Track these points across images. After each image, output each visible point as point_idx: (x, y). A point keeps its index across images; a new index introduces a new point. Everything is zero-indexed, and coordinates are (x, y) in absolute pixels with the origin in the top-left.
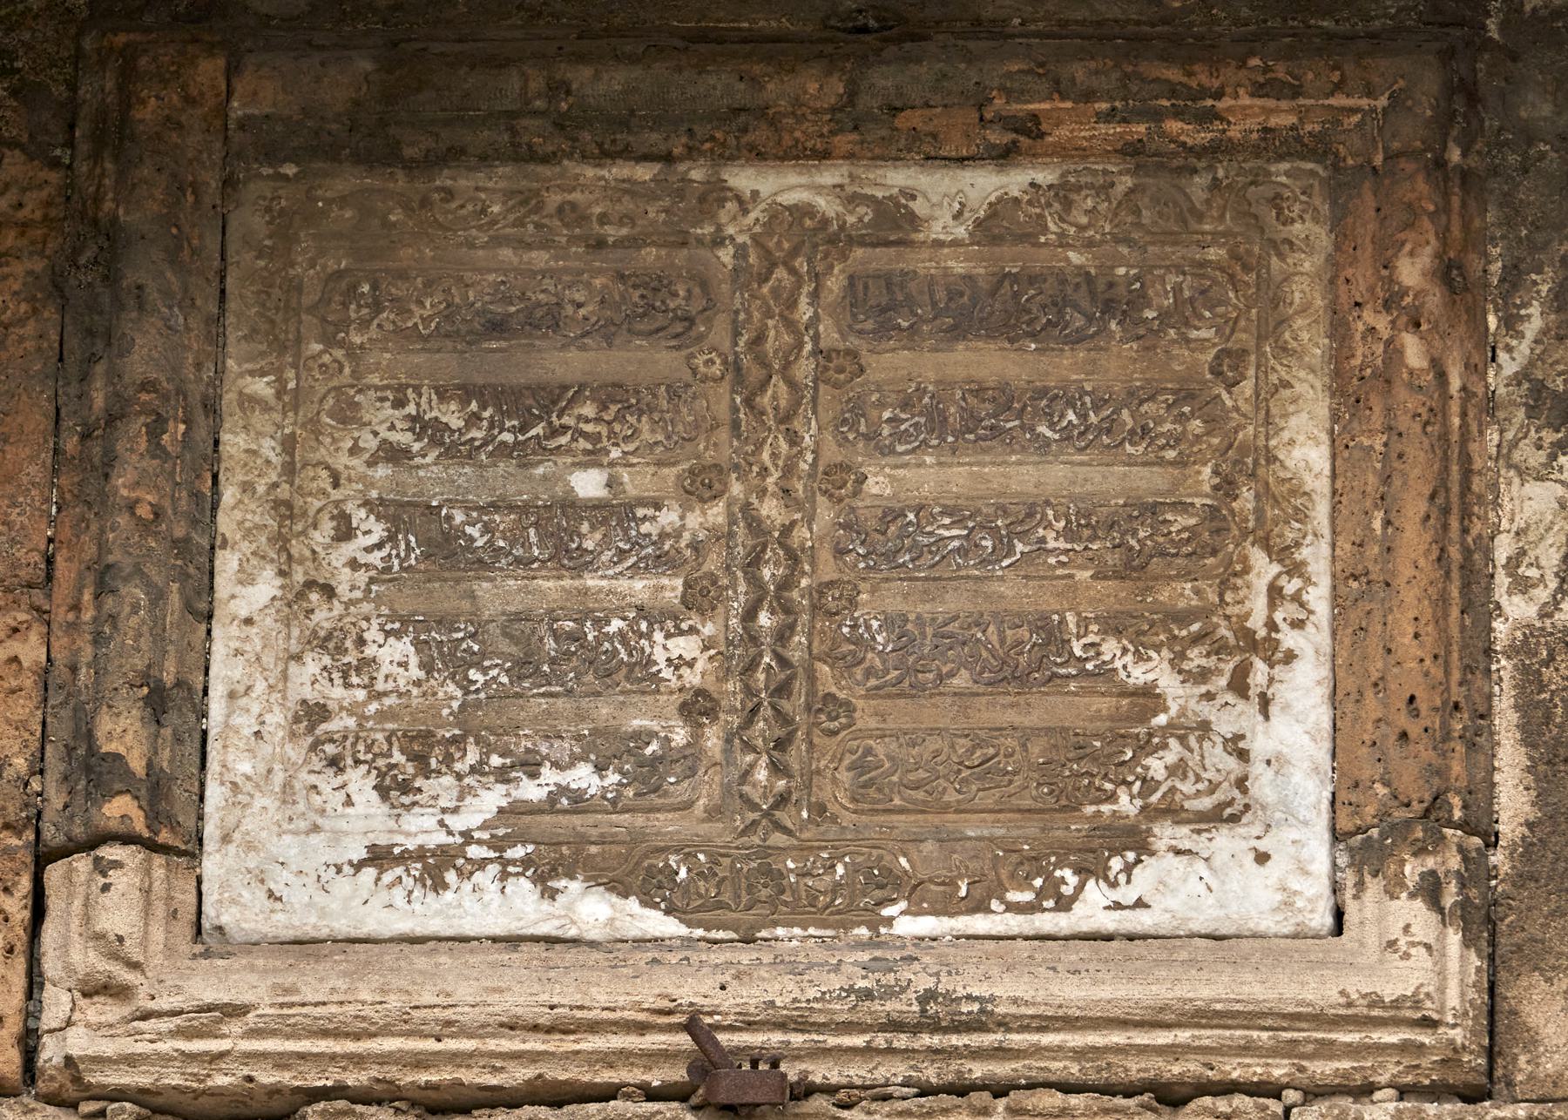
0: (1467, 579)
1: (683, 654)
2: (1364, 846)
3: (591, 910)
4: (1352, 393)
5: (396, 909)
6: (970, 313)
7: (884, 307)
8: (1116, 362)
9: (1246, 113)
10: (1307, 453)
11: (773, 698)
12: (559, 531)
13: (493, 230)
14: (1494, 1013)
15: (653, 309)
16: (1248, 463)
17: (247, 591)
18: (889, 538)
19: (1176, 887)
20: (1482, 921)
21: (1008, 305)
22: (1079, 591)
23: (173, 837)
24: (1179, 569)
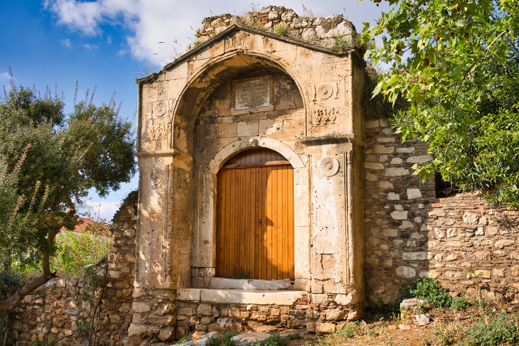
0: (274, 93)
1: (250, 98)
2: (270, 103)
3: (247, 108)
4: (270, 86)
5: (241, 108)
6: (258, 85)
7: (256, 85)
8: (263, 86)
9: (267, 77)
10: (269, 89)
11: (252, 100)
12: (246, 95)
13: (244, 84)
14: (275, 108)
15: (249, 86)
16: (267, 89)
17: (237, 98)
18: (256, 94)
19: (265, 105)
20: (274, 105)
21: (260, 85)
22: (261, 94)
23: (234, 106)
24: (264, 94)
